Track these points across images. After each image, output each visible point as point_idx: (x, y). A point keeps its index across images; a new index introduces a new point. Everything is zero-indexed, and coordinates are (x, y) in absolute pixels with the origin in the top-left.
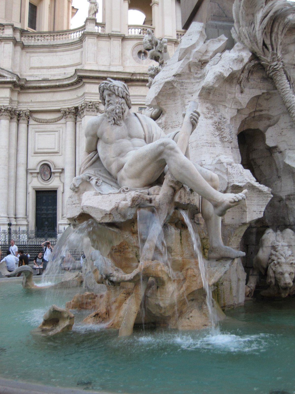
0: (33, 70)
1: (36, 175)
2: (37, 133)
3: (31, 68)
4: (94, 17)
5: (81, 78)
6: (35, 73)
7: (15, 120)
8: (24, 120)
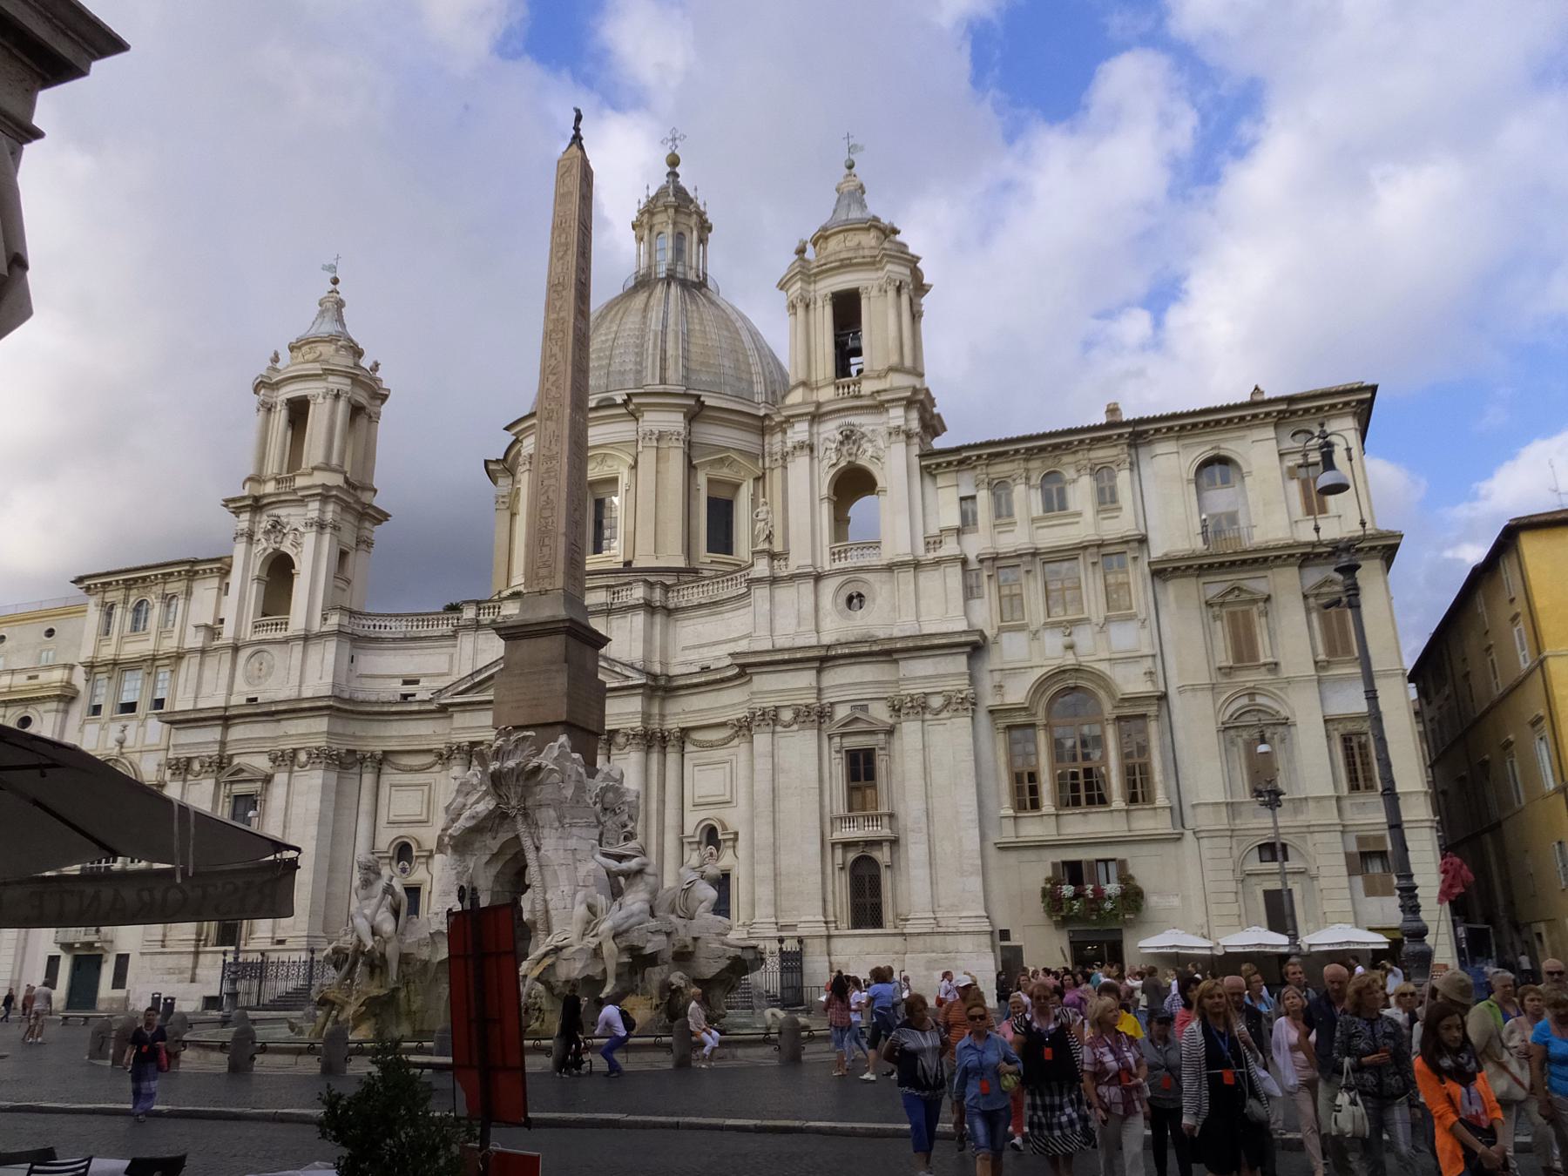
0: (687, 652)
1: (695, 846)
2: (696, 768)
3: (685, 649)
4: (766, 546)
5: (743, 667)
6: (692, 657)
7: (656, 748)
8: (673, 746)
